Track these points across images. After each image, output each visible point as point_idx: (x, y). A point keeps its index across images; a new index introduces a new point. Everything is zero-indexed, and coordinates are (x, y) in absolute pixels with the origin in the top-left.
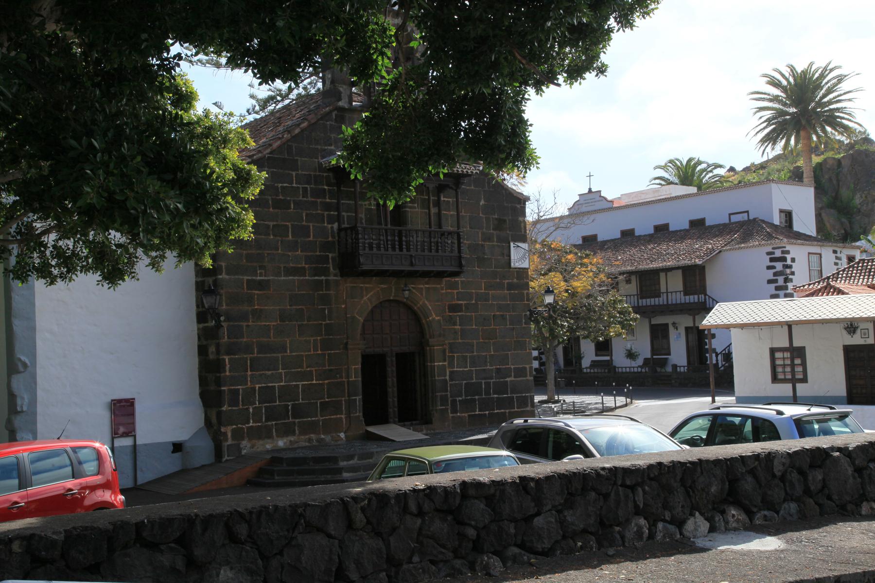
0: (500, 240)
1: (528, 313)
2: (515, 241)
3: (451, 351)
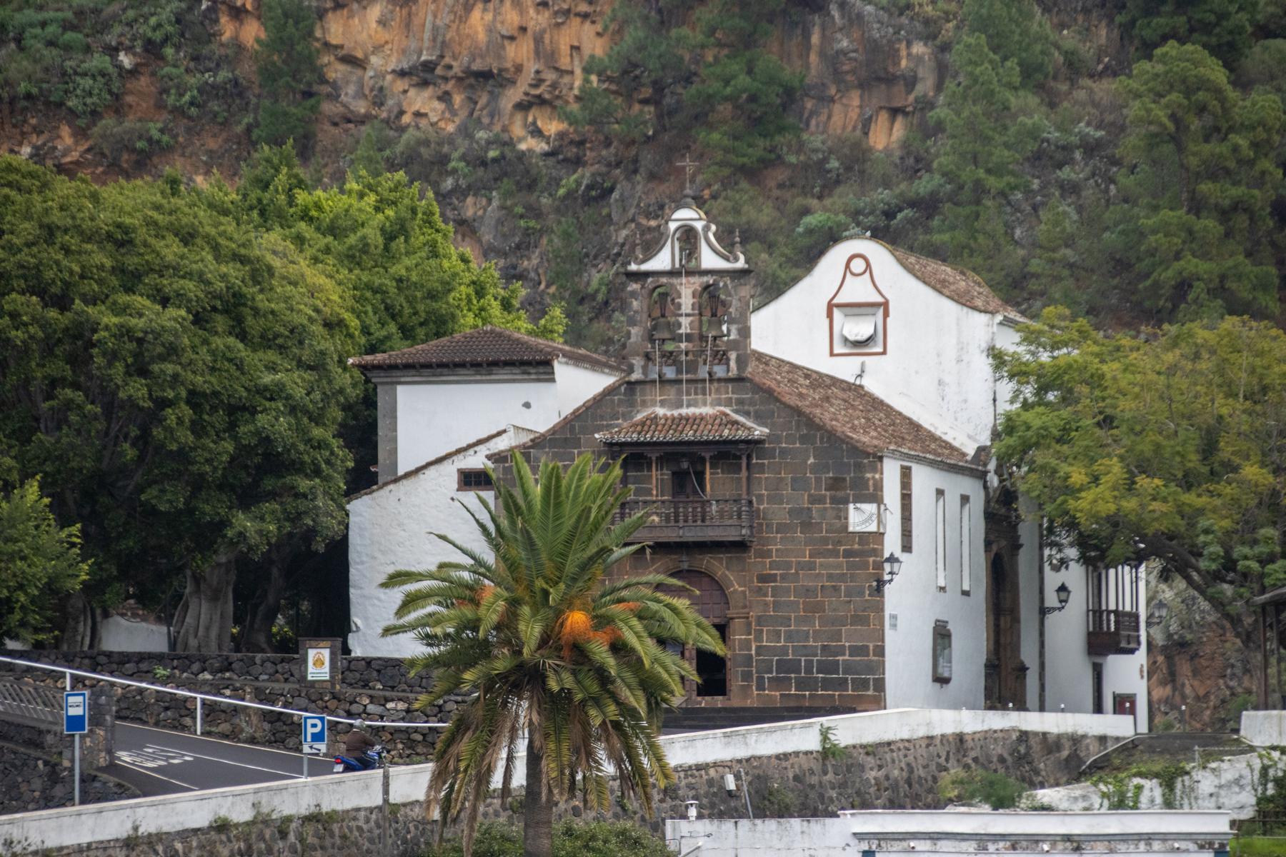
0: (834, 500)
1: (875, 584)
2: (855, 502)
3: (759, 624)
